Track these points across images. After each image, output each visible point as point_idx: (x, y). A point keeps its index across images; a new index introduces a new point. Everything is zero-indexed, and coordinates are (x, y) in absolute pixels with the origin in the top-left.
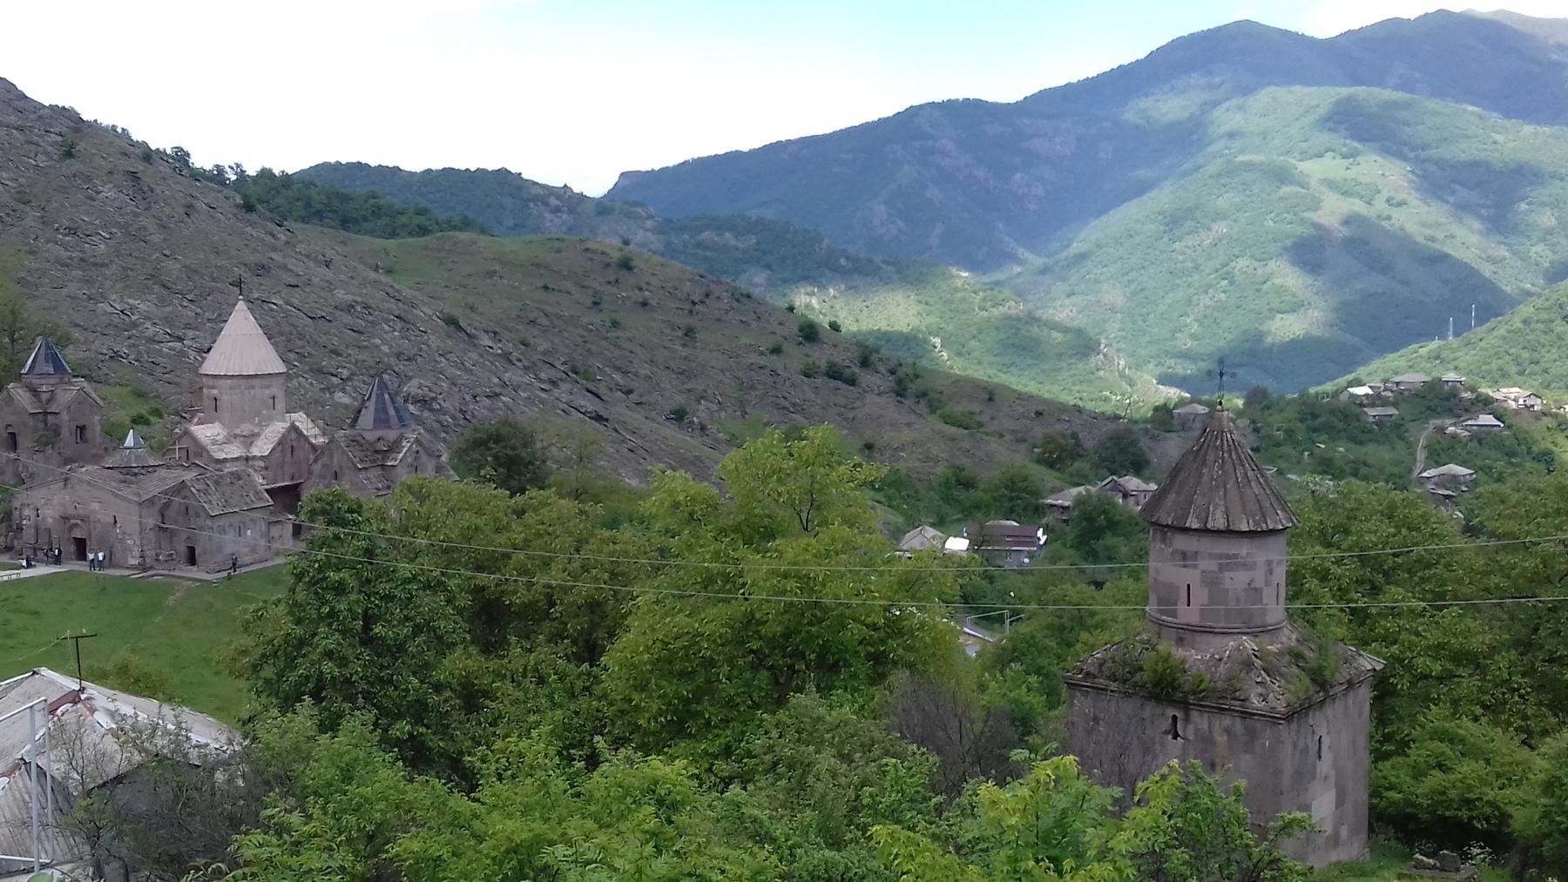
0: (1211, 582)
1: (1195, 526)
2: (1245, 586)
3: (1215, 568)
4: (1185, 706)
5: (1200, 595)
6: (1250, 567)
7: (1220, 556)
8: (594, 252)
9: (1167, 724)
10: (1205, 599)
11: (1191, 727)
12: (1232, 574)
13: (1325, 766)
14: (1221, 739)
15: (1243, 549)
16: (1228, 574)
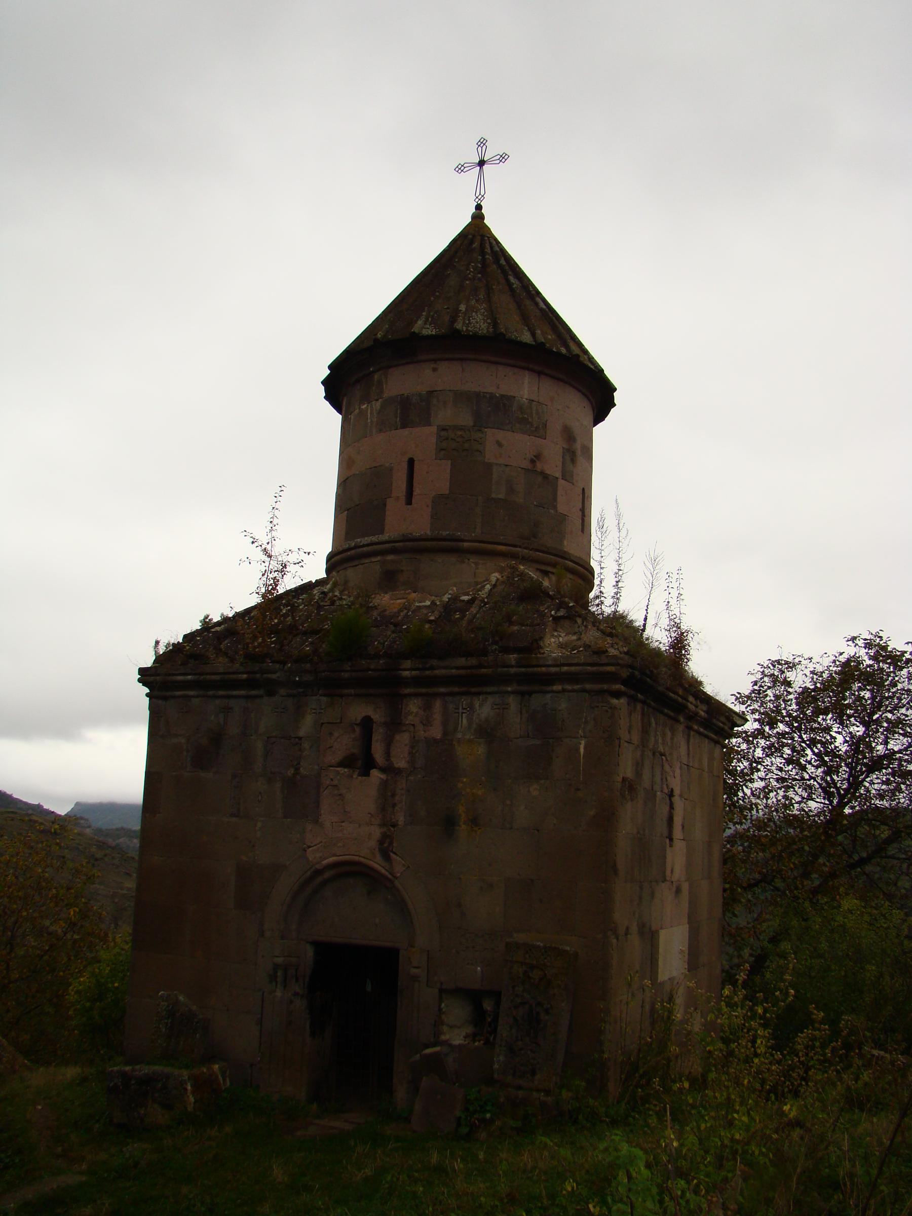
0: (458, 449)
1: (429, 331)
2: (526, 464)
3: (466, 419)
4: (388, 688)
5: (435, 478)
6: (539, 430)
7: (473, 399)
8: (36, 822)
9: (343, 743)
10: (444, 486)
11: (403, 739)
12: (500, 435)
13: (677, 859)
14: (471, 753)
15: (524, 387)
16: (492, 435)
